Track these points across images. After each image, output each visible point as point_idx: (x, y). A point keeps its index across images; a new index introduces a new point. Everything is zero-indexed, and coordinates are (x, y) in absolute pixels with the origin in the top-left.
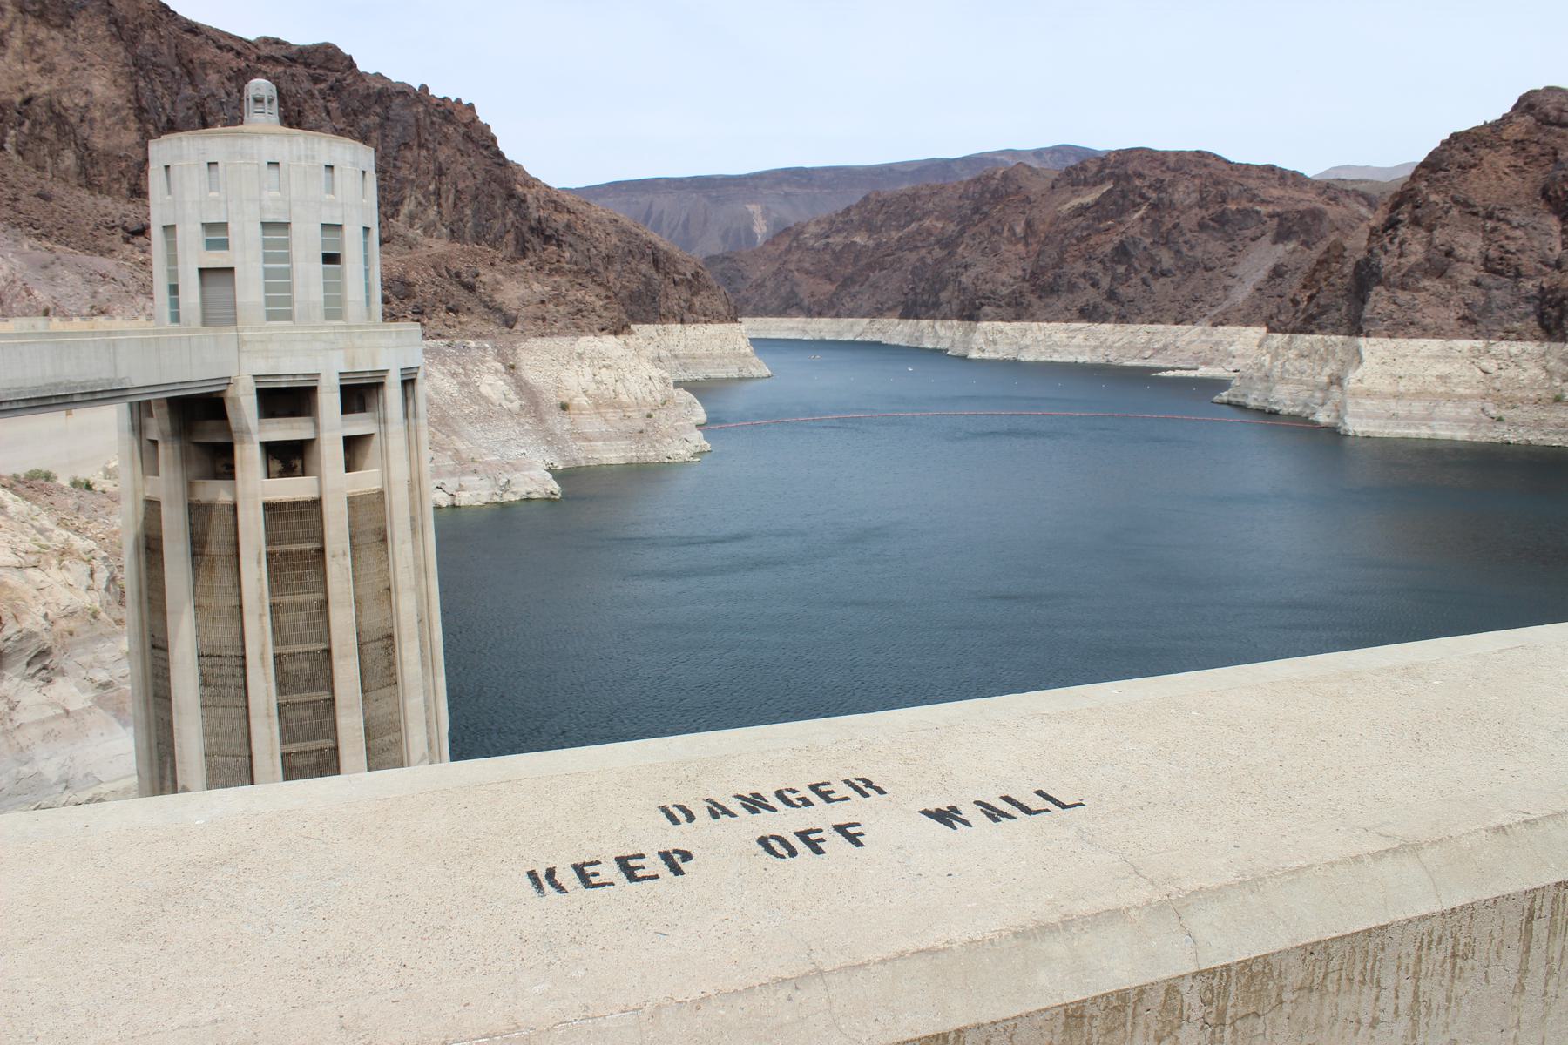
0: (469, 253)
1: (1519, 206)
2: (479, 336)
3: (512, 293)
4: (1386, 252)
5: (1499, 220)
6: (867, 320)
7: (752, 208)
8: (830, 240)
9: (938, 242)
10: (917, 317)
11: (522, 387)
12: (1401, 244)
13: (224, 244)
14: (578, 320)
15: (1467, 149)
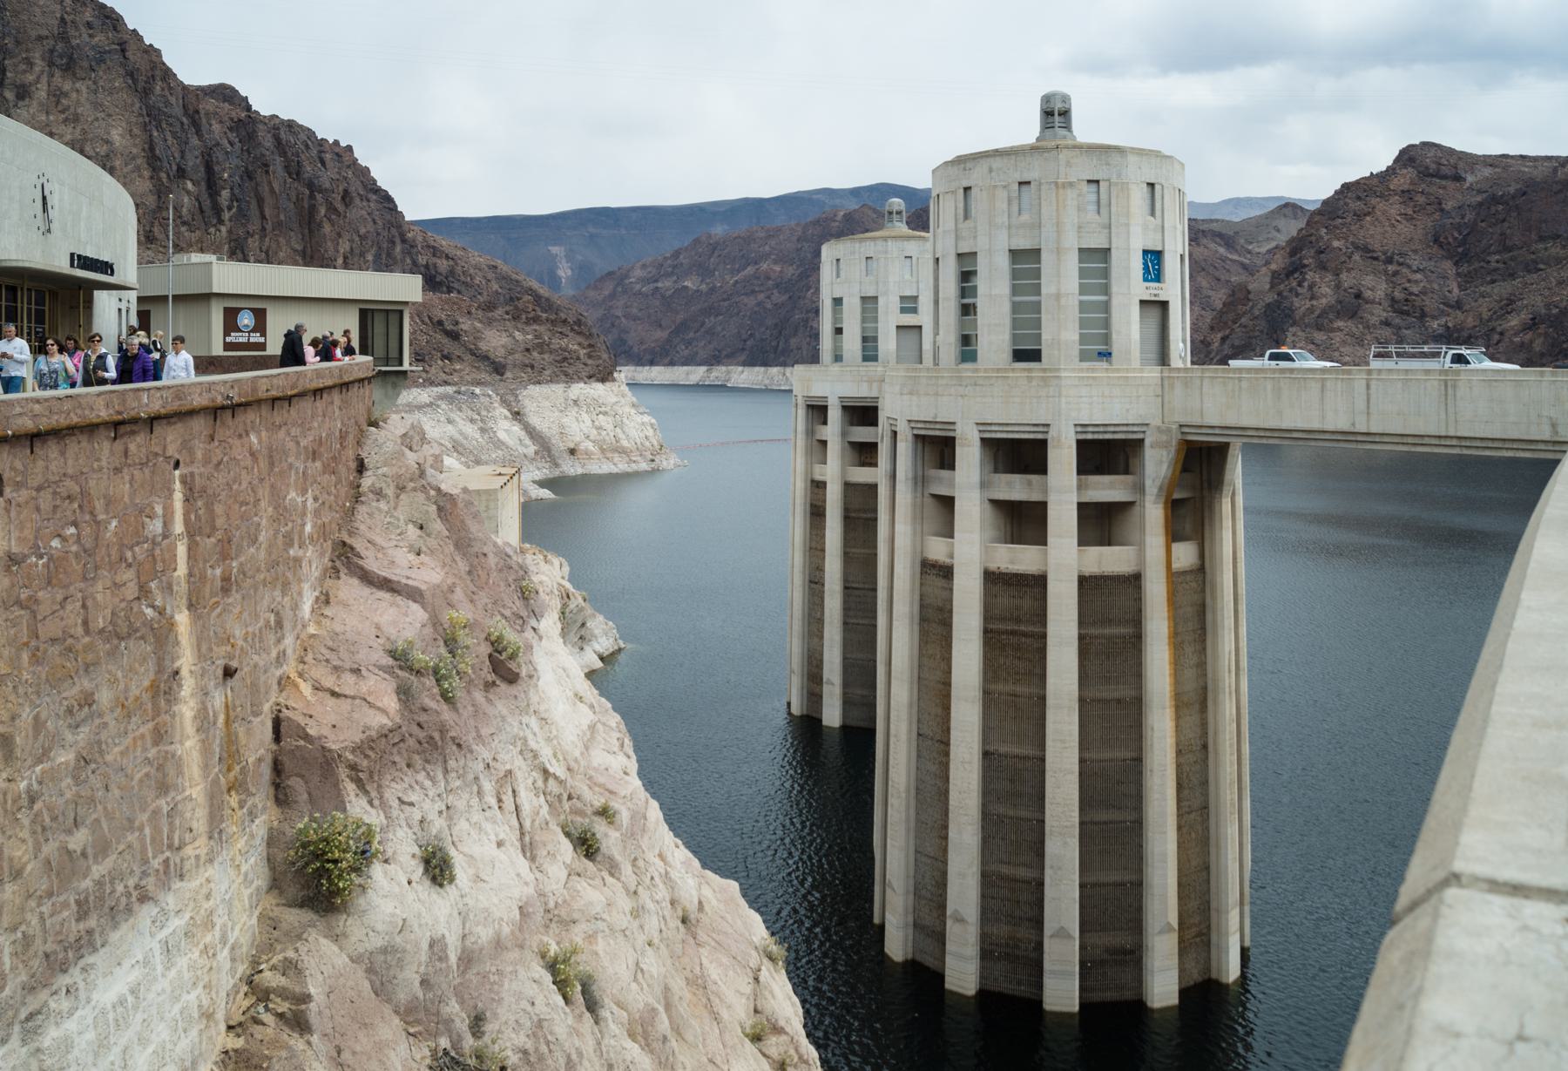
0: (447, 302)
1: (1415, 251)
2: (479, 383)
3: (495, 341)
4: (1297, 295)
5: (1400, 264)
6: (704, 368)
7: (555, 250)
8: (660, 285)
9: (777, 286)
10: (765, 364)
11: (532, 433)
12: (1311, 287)
13: (914, 310)
14: (565, 369)
15: (1359, 198)
